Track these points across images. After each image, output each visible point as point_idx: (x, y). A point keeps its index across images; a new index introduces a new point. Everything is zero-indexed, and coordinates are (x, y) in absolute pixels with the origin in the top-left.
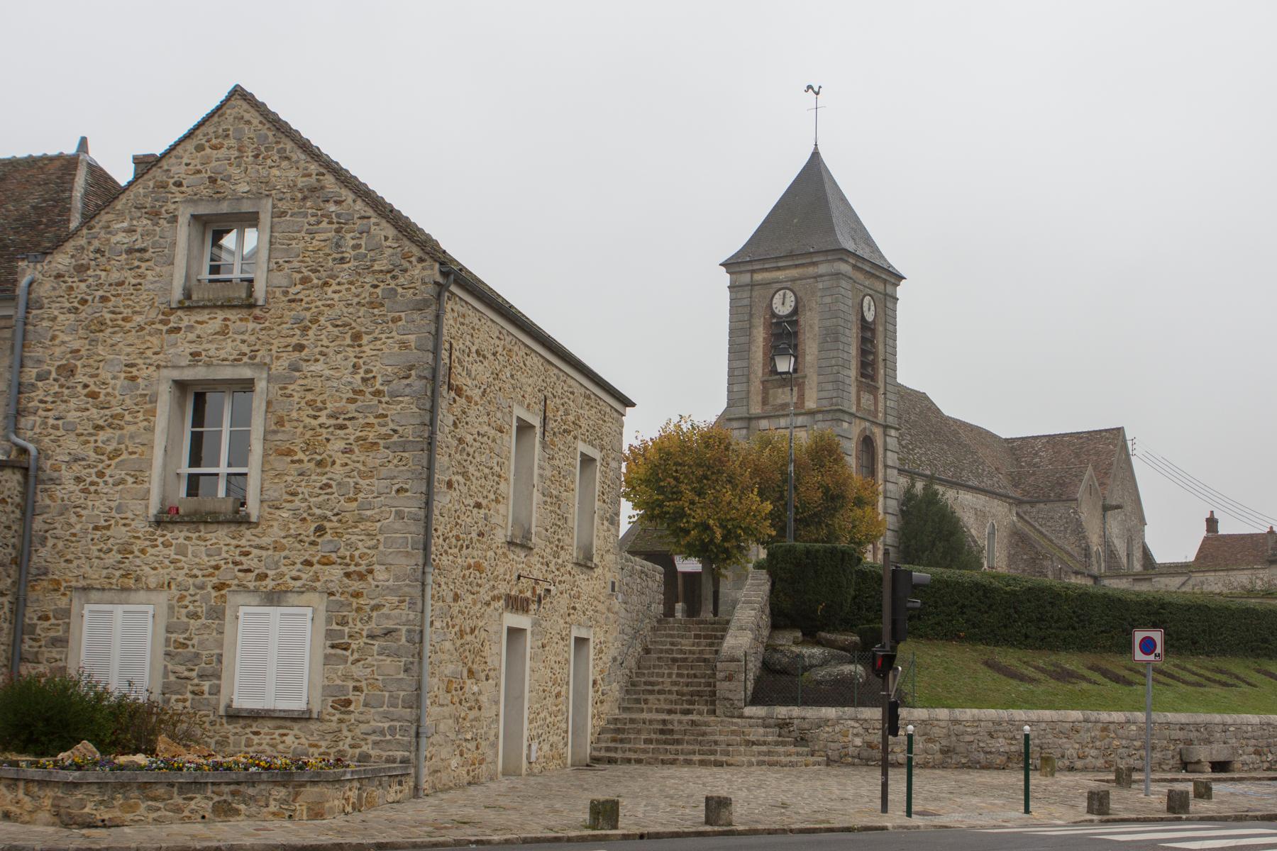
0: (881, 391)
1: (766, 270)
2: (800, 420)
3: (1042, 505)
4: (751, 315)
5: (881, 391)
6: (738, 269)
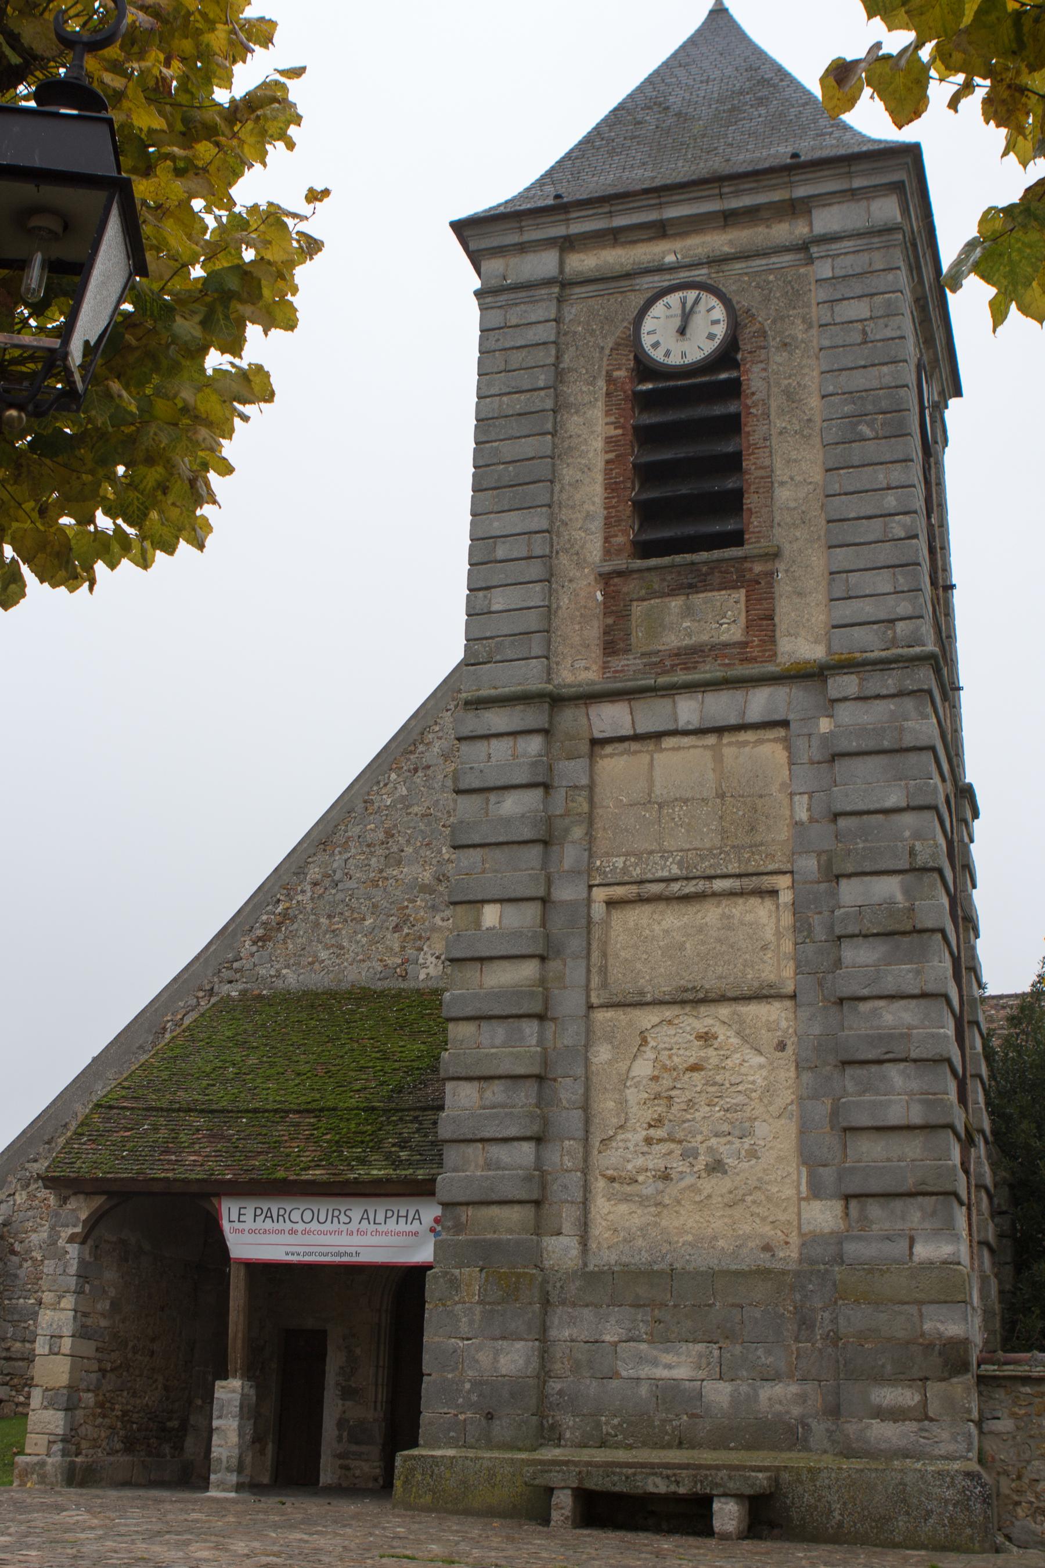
1: (614, 237)
2: (759, 703)
4: (560, 375)
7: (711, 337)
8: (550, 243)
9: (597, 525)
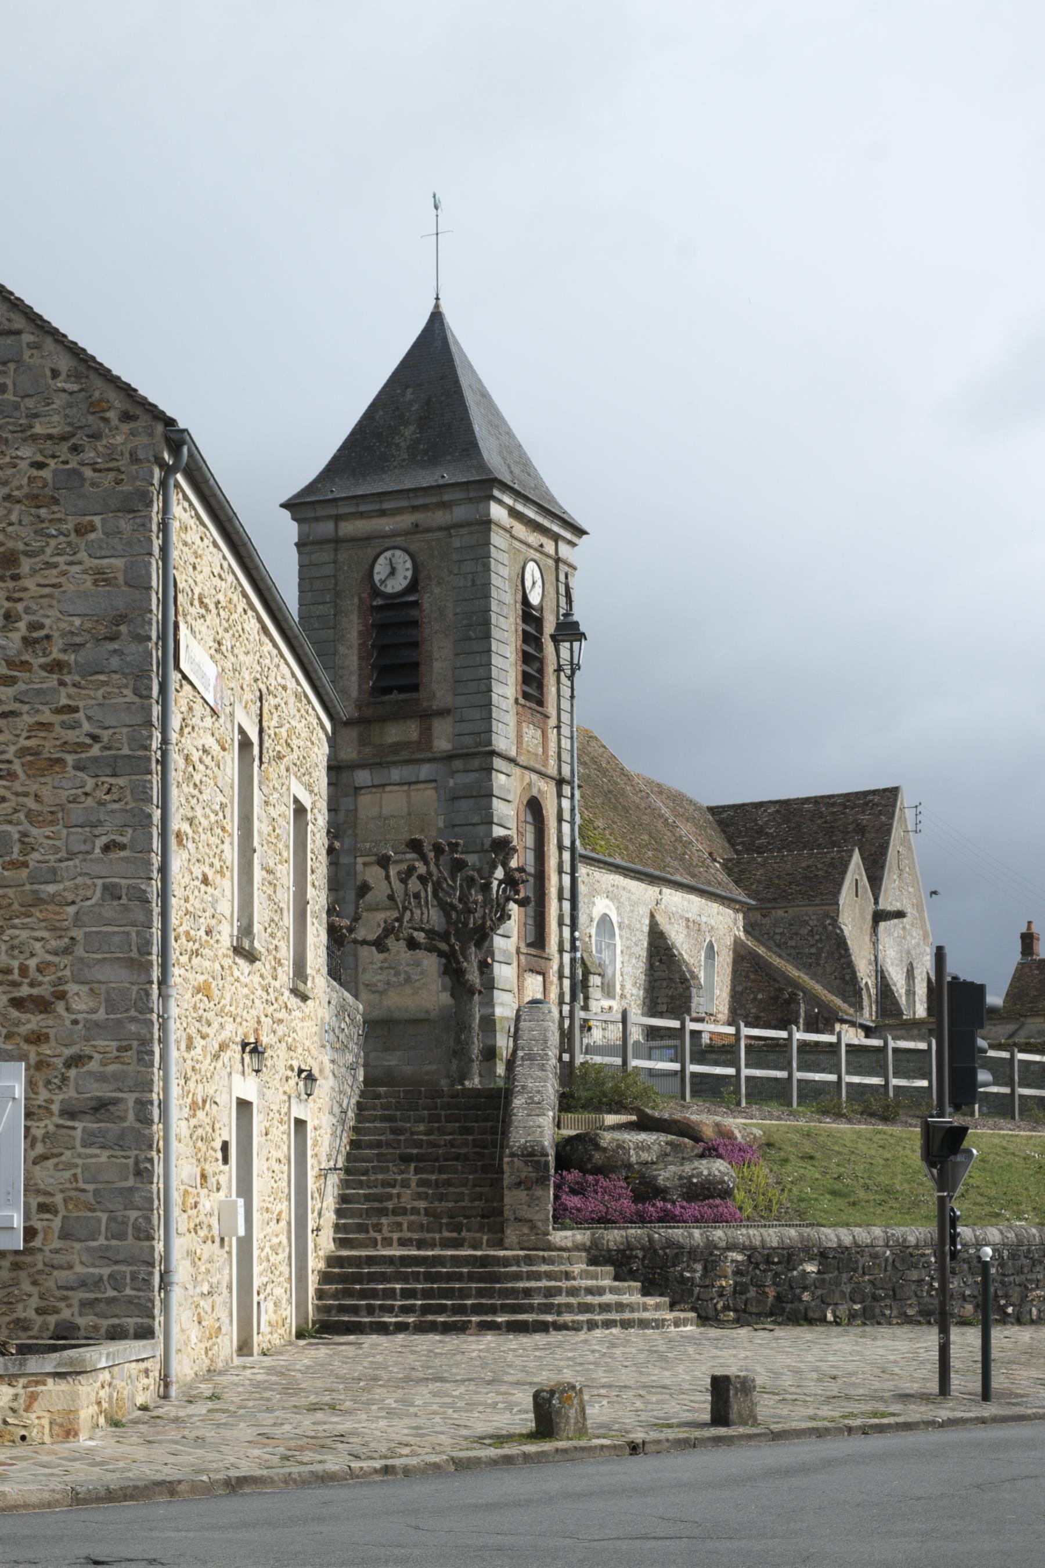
0: (553, 722)
1: (362, 515)
2: (425, 771)
3: (780, 913)
5: (553, 722)
6: (311, 514)
7: (405, 578)
8: (329, 517)
9: (354, 678)
